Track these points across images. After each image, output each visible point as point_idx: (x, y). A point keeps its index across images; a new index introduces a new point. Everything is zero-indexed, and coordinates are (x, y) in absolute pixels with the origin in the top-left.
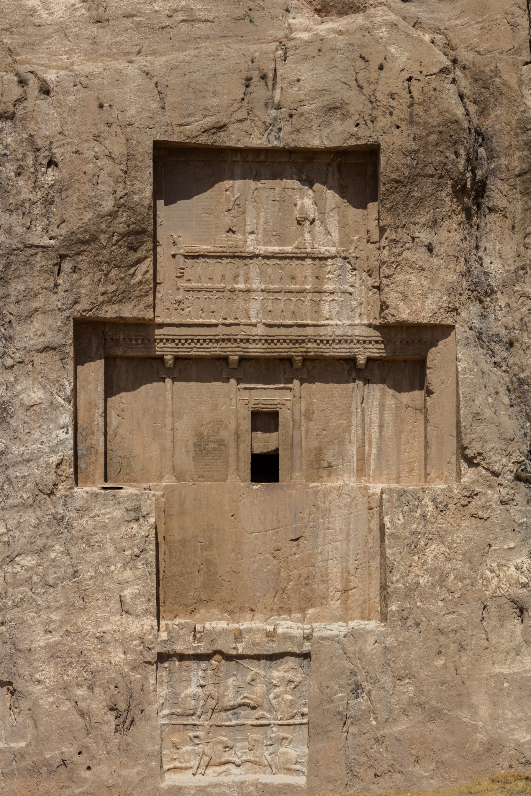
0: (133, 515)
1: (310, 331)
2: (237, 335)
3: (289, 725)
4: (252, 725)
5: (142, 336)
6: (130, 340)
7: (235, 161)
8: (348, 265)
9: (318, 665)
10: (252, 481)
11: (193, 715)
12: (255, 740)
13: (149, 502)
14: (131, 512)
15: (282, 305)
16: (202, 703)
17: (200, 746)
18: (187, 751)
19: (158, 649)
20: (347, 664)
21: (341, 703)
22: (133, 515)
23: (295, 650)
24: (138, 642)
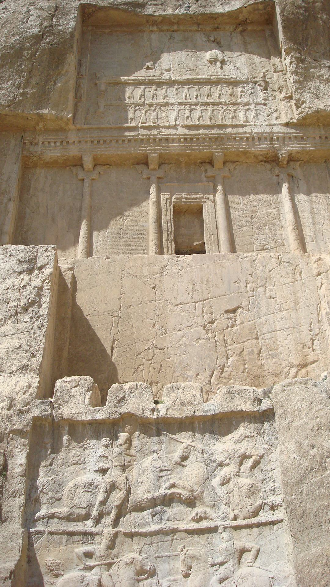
0: (25, 266)
1: (229, 130)
3: (250, 526)
4: (187, 531)
5: (61, 138)
6: (49, 143)
7: (152, 31)
8: (259, 87)
9: (288, 421)
11: (87, 517)
12: (192, 557)
13: (47, 254)
14: (23, 264)
15: (198, 113)
16: (101, 496)
17: (94, 570)
18: (71, 580)
19: (36, 412)
22: (25, 266)
23: (248, 407)
24: (6, 403)
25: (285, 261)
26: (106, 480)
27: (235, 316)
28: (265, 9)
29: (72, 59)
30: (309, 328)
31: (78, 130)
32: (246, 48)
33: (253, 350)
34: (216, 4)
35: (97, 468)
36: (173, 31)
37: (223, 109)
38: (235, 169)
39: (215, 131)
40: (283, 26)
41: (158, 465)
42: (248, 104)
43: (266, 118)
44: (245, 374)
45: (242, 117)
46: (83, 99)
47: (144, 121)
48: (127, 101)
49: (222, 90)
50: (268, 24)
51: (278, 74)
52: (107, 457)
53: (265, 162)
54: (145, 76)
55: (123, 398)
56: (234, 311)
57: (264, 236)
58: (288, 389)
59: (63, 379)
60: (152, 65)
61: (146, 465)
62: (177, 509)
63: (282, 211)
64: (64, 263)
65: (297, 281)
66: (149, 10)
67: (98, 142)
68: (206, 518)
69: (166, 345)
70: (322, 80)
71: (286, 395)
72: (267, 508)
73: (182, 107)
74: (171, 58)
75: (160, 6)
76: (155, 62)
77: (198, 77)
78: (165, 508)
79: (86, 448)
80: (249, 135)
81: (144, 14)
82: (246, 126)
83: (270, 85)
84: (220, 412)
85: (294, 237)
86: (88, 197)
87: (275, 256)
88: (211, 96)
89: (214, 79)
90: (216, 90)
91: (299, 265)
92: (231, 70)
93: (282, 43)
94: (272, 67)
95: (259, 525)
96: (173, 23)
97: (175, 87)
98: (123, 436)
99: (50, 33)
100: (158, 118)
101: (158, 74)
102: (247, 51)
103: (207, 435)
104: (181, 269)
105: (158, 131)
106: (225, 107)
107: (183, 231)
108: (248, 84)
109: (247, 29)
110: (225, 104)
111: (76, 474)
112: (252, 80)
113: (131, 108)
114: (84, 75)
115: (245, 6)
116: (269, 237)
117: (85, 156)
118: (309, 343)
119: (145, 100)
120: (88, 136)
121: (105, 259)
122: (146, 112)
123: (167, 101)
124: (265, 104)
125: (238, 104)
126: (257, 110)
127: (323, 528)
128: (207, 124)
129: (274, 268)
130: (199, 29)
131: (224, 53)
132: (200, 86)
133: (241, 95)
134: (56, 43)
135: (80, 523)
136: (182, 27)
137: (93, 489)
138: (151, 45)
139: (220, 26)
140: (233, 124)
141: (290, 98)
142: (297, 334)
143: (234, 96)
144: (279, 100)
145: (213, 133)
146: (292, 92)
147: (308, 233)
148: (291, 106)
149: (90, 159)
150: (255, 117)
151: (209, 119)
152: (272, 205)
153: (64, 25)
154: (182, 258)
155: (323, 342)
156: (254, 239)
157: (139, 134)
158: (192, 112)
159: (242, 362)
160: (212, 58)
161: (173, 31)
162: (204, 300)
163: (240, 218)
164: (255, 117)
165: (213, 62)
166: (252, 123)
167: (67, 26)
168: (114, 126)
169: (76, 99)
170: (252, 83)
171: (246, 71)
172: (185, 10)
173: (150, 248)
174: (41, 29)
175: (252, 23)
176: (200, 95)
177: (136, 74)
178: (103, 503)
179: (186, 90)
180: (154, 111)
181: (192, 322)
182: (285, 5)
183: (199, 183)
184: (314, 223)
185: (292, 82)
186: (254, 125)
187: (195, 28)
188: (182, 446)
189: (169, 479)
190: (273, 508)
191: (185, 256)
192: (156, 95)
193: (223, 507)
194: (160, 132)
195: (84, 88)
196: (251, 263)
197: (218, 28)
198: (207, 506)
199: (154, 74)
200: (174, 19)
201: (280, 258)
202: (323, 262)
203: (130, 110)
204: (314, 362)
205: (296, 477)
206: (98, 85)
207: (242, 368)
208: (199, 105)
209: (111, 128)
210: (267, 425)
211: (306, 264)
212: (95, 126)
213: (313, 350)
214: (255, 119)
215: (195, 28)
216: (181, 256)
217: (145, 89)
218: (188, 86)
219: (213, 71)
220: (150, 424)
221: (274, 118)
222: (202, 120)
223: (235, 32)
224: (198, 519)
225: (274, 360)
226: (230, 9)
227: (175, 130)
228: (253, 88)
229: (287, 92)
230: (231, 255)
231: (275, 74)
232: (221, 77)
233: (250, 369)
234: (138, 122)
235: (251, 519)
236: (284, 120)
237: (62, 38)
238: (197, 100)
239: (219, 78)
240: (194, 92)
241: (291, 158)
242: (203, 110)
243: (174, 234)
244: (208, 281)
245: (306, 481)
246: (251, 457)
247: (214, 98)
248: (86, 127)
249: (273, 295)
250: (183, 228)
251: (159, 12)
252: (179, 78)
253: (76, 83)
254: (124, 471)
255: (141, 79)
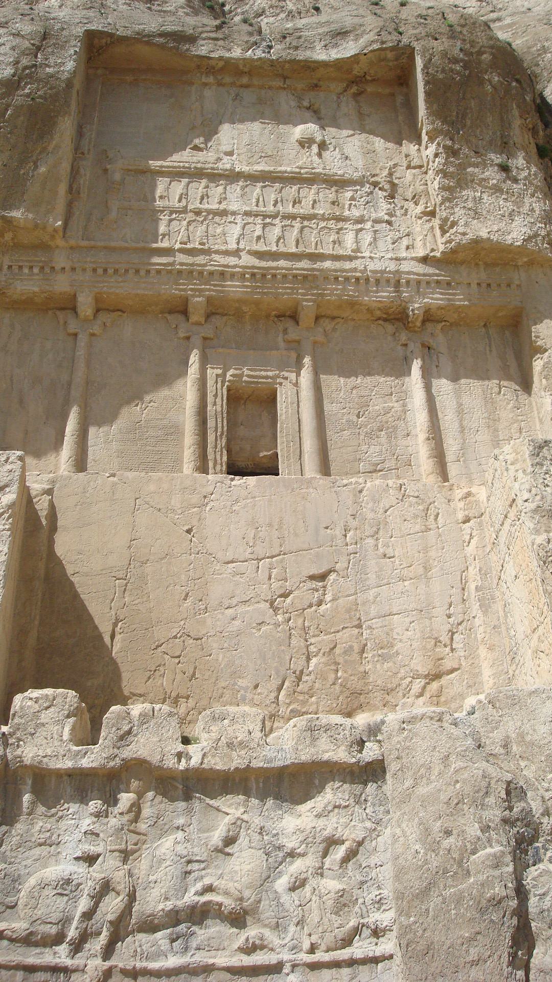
1: (328, 264)
2: (205, 265)
3: (336, 965)
4: (231, 970)
6: (21, 267)
7: (205, 84)
8: (380, 192)
9: (408, 784)
10: (229, 473)
11: (59, 939)
13: (9, 467)
16: (84, 904)
20: (492, 771)
21: (497, 873)
23: (341, 755)
25: (412, 494)
26: (95, 875)
27: (324, 587)
28: (397, 59)
29: (66, 126)
30: (448, 612)
31: (71, 248)
32: (361, 124)
33: (351, 647)
34: (315, 44)
35: (79, 854)
36: (241, 86)
37: (319, 227)
38: (334, 330)
39: (304, 264)
40: (425, 92)
41: (185, 852)
42: (361, 220)
43: (391, 246)
44: (337, 687)
45: (349, 242)
46: (82, 195)
47: (185, 239)
48: (158, 203)
49: (318, 193)
50: (401, 84)
51: (414, 171)
52: (97, 835)
53: (385, 320)
54: (191, 161)
55: (129, 732)
56: (323, 577)
57: (378, 448)
58: (409, 727)
59: (26, 694)
60: (202, 143)
61: (163, 850)
62: (214, 929)
63: (409, 407)
64: (36, 481)
65: (430, 529)
66: (203, 48)
67: (105, 271)
68: (262, 947)
69: (204, 632)
70: (486, 187)
71: (406, 738)
72: (366, 932)
73: (251, 220)
74: (236, 132)
75: (221, 43)
76: (207, 140)
77: (279, 169)
78: (194, 928)
79: (61, 817)
80: (360, 275)
81: (194, 55)
82: (357, 258)
83: (400, 191)
84: (293, 764)
85: (428, 453)
86: (83, 365)
87: (394, 486)
88: (300, 202)
89: (306, 173)
90: (309, 194)
91: (434, 502)
92: (336, 160)
93: (422, 120)
94: (404, 159)
95: (352, 963)
96: (242, 73)
97: (241, 183)
98: (126, 799)
99: (31, 78)
100: (209, 235)
101: (212, 159)
102: (363, 130)
103: (270, 802)
104: (237, 501)
105: (208, 257)
106: (322, 224)
107: (242, 431)
108: (362, 187)
109: (365, 90)
110: (323, 218)
111: (42, 862)
112: (369, 180)
113: (164, 216)
114: (86, 152)
115: (364, 51)
116: (387, 450)
117: (81, 295)
118: (445, 638)
119: (187, 203)
120: (88, 259)
121: (108, 477)
122: (189, 223)
123: (225, 207)
124: (389, 223)
125: (345, 219)
126: (375, 232)
127: (460, 975)
128: (290, 251)
129: (393, 506)
130: (285, 86)
131: (325, 130)
132: (281, 185)
133: (350, 205)
134: (40, 97)
135: (47, 950)
136: (256, 82)
137: (71, 891)
138: (202, 107)
139: (321, 83)
140: (335, 253)
141: (432, 214)
142: (427, 622)
143: (338, 205)
144: (413, 216)
145: (301, 266)
146: (435, 204)
147: (451, 447)
148: (432, 228)
149: (90, 300)
150: (371, 243)
151: (294, 243)
152: (394, 395)
153: (57, 65)
154: (238, 481)
155: (469, 636)
156: (360, 452)
157: (175, 261)
158: (267, 229)
159: (333, 667)
160: (305, 137)
161: (241, 86)
162: (272, 557)
163: (340, 415)
164: (371, 243)
165: (307, 145)
166: (367, 254)
167: (62, 69)
168: (134, 245)
169: (71, 194)
170: (370, 184)
171: (360, 164)
172: (264, 52)
173: (185, 460)
174: (17, 69)
175: (374, 80)
176: (282, 201)
177: (176, 157)
178: (88, 915)
179: (258, 190)
180: (202, 222)
181: (250, 594)
182: (431, 55)
183: (273, 351)
184: (462, 429)
185: (437, 189)
186: (371, 257)
187: (279, 83)
188: (227, 819)
189: (202, 878)
190: (377, 933)
191: (245, 478)
192: (207, 195)
193: (292, 929)
194: (211, 260)
195: (85, 175)
196: (355, 495)
197: (316, 86)
198: (265, 926)
199: (206, 158)
200: (245, 66)
201: (403, 489)
202: (475, 499)
203: (161, 219)
204: (453, 671)
205: (418, 885)
206: (109, 172)
207: (332, 676)
208: (279, 217)
209: (127, 249)
210: (371, 788)
211: (447, 501)
212: (99, 244)
213: (452, 650)
214: (372, 247)
215: (279, 83)
216: (237, 478)
217: (189, 183)
218: (261, 184)
219: (304, 160)
220: (173, 778)
221: (404, 247)
222: (283, 244)
223: (345, 93)
224: (250, 949)
225: (386, 665)
226: (339, 56)
227: (236, 259)
228: (372, 193)
229: (427, 203)
230: (321, 481)
231: (409, 171)
232: (317, 171)
233: (346, 679)
234: (174, 241)
235: (339, 952)
236: (421, 251)
237: (51, 89)
238: (277, 209)
239: (314, 173)
240: (271, 195)
241: (429, 317)
242: (286, 226)
243: (227, 436)
244: (281, 523)
245: (434, 893)
246: (343, 842)
247: (304, 207)
248: (84, 243)
249: (390, 552)
250: (242, 427)
251: (219, 52)
252: (248, 168)
253: (72, 165)
254: (125, 861)
255: (184, 167)
